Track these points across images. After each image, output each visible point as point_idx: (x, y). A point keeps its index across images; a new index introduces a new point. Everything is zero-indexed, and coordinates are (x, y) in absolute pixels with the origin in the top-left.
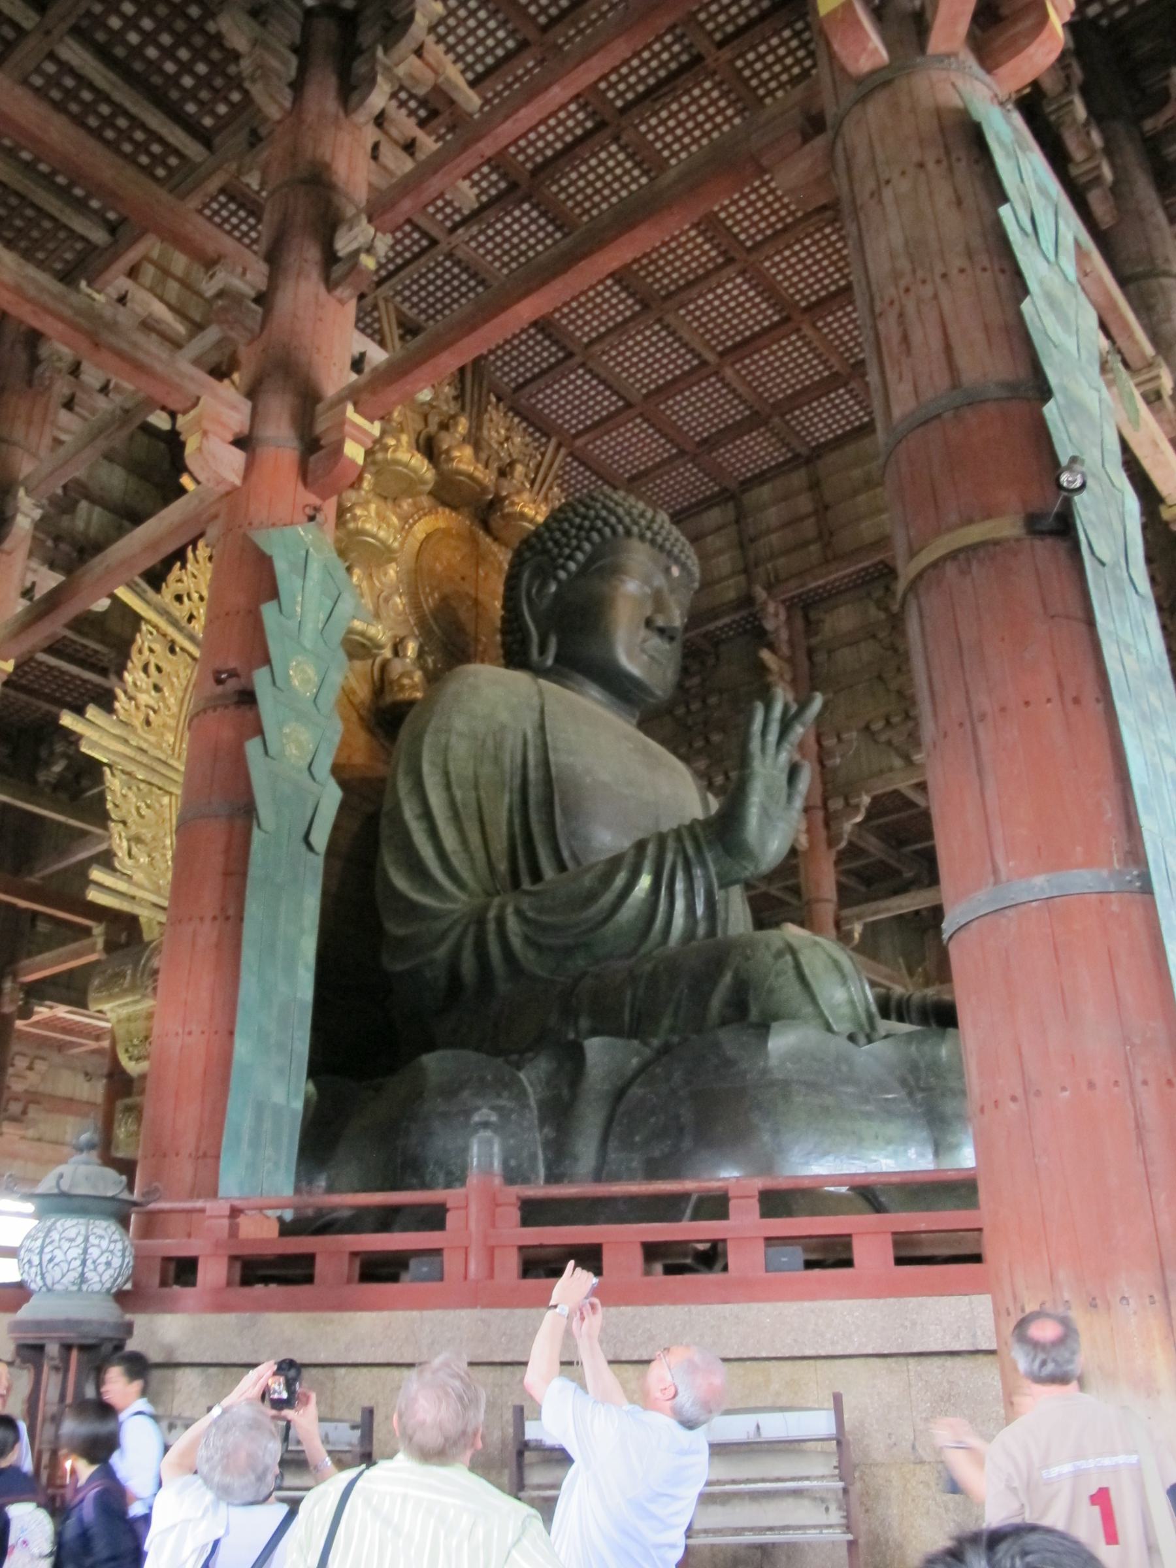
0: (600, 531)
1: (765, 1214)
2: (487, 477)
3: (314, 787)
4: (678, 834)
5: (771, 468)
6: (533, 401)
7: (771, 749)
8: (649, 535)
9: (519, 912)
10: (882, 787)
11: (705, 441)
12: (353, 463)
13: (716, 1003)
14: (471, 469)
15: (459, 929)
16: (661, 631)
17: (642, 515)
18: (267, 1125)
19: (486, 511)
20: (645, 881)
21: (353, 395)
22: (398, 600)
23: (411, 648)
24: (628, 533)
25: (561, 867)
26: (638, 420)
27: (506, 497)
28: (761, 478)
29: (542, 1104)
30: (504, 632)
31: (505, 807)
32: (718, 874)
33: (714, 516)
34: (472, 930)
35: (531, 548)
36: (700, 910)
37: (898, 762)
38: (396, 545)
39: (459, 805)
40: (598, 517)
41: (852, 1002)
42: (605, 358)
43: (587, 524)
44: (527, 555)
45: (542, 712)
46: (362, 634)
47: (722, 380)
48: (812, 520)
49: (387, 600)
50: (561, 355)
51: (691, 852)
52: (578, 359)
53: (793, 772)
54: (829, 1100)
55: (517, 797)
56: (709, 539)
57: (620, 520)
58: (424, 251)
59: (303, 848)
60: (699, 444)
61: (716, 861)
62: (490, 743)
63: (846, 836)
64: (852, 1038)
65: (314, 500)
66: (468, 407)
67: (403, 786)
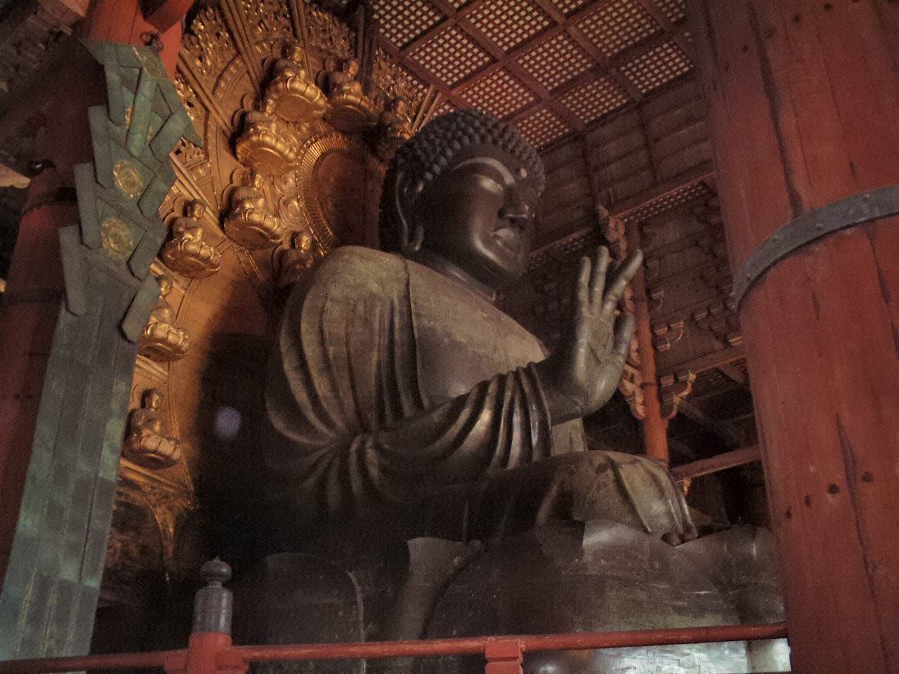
0: (460, 140)
4: (516, 374)
5: (610, 112)
9: (377, 447)
10: (707, 365)
11: (556, 90)
13: (542, 515)
14: (359, 100)
15: (327, 461)
16: (513, 221)
17: (495, 126)
18: (52, 601)
22: (296, 204)
23: (305, 241)
28: (603, 120)
32: (550, 409)
33: (566, 151)
34: (337, 461)
35: (404, 156)
36: (535, 440)
37: (718, 345)
39: (331, 357)
41: (669, 513)
42: (473, 21)
44: (401, 161)
45: (408, 285)
46: (260, 225)
49: (286, 203)
50: (437, 18)
51: (527, 389)
52: (451, 21)
53: (618, 324)
54: (642, 596)
55: (385, 355)
56: (561, 171)
59: (116, 335)
60: (551, 93)
61: (549, 397)
62: (361, 308)
63: (676, 407)
66: (360, 56)
67: (284, 342)
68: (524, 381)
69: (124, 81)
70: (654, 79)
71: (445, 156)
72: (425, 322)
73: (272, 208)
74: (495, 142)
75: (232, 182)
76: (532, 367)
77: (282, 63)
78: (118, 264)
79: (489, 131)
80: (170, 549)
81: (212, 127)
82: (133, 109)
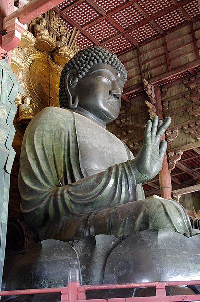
1: (168, 294)
2: (53, 41)
4: (122, 164)
6: (68, 14)
7: (154, 137)
9: (69, 192)
14: (48, 38)
16: (114, 95)
17: (107, 55)
19: (53, 53)
20: (112, 181)
21: (17, 15)
23: (28, 100)
24: (103, 61)
25: (82, 177)
26: (104, 21)
27: (60, 48)
28: (146, 42)
29: (81, 257)
30: (60, 96)
31: (62, 156)
33: (129, 55)
34: (52, 198)
35: (69, 67)
37: (193, 140)
40: (92, 56)
43: (89, 58)
44: (69, 69)
45: (75, 124)
48: (164, 56)
51: (127, 172)
53: (161, 144)
55: (66, 153)
56: (128, 63)
57: (100, 57)
62: (57, 134)
63: (175, 165)
64: (185, 235)
70: (169, 25)
74: (107, 62)
79: (105, 58)
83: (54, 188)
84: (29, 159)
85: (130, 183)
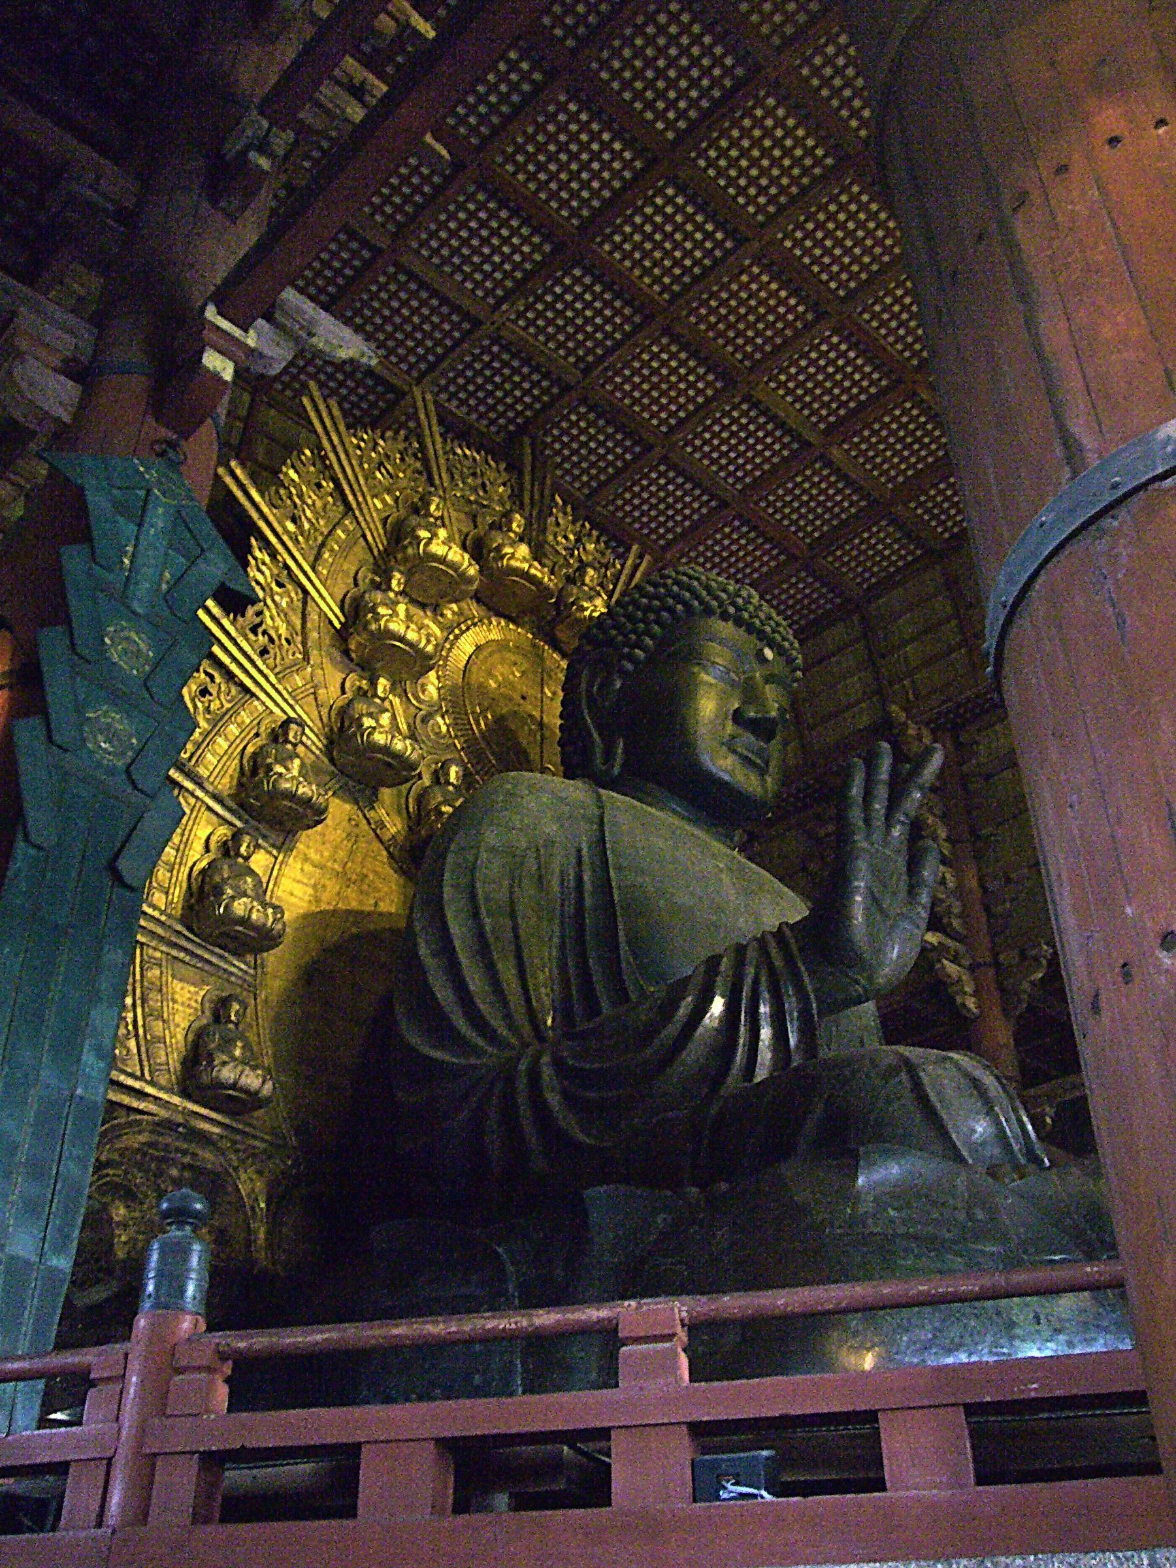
0: (671, 610)
3: (136, 798)
4: (761, 941)
6: (611, 508)
8: (732, 610)
9: (558, 1063)
12: (216, 377)
14: (526, 566)
20: (718, 1006)
22: (439, 719)
23: (454, 772)
28: (887, 583)
32: (816, 990)
33: (837, 634)
34: (498, 1087)
38: (430, 648)
40: (669, 593)
45: (601, 823)
46: (386, 750)
47: (829, 464)
49: (425, 720)
51: (778, 963)
52: (658, 451)
58: (466, 335)
61: (812, 973)
65: (164, 433)
68: (774, 952)
69: (121, 508)
71: (652, 637)
72: (631, 878)
73: (404, 727)
75: (343, 692)
76: (788, 932)
77: (414, 520)
78: (111, 771)
80: (262, 1235)
81: (314, 616)
82: (135, 546)
83: (507, 1054)
84: (423, 951)
85: (791, 1004)
